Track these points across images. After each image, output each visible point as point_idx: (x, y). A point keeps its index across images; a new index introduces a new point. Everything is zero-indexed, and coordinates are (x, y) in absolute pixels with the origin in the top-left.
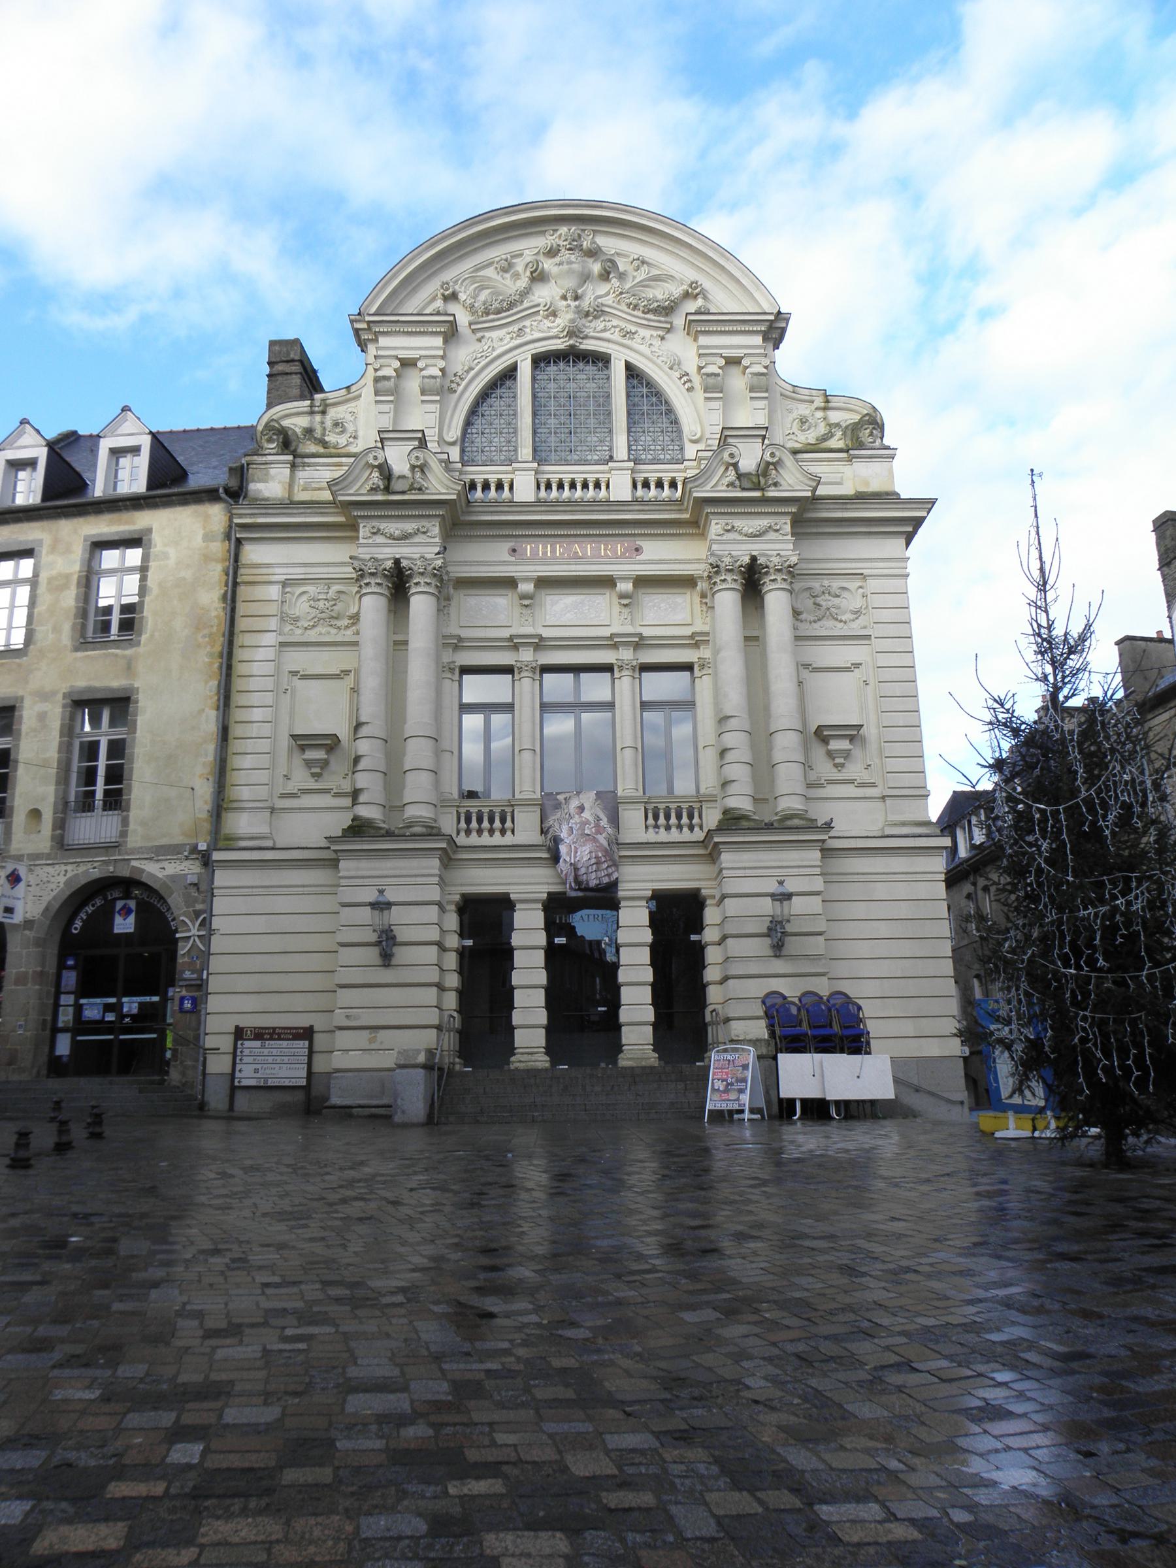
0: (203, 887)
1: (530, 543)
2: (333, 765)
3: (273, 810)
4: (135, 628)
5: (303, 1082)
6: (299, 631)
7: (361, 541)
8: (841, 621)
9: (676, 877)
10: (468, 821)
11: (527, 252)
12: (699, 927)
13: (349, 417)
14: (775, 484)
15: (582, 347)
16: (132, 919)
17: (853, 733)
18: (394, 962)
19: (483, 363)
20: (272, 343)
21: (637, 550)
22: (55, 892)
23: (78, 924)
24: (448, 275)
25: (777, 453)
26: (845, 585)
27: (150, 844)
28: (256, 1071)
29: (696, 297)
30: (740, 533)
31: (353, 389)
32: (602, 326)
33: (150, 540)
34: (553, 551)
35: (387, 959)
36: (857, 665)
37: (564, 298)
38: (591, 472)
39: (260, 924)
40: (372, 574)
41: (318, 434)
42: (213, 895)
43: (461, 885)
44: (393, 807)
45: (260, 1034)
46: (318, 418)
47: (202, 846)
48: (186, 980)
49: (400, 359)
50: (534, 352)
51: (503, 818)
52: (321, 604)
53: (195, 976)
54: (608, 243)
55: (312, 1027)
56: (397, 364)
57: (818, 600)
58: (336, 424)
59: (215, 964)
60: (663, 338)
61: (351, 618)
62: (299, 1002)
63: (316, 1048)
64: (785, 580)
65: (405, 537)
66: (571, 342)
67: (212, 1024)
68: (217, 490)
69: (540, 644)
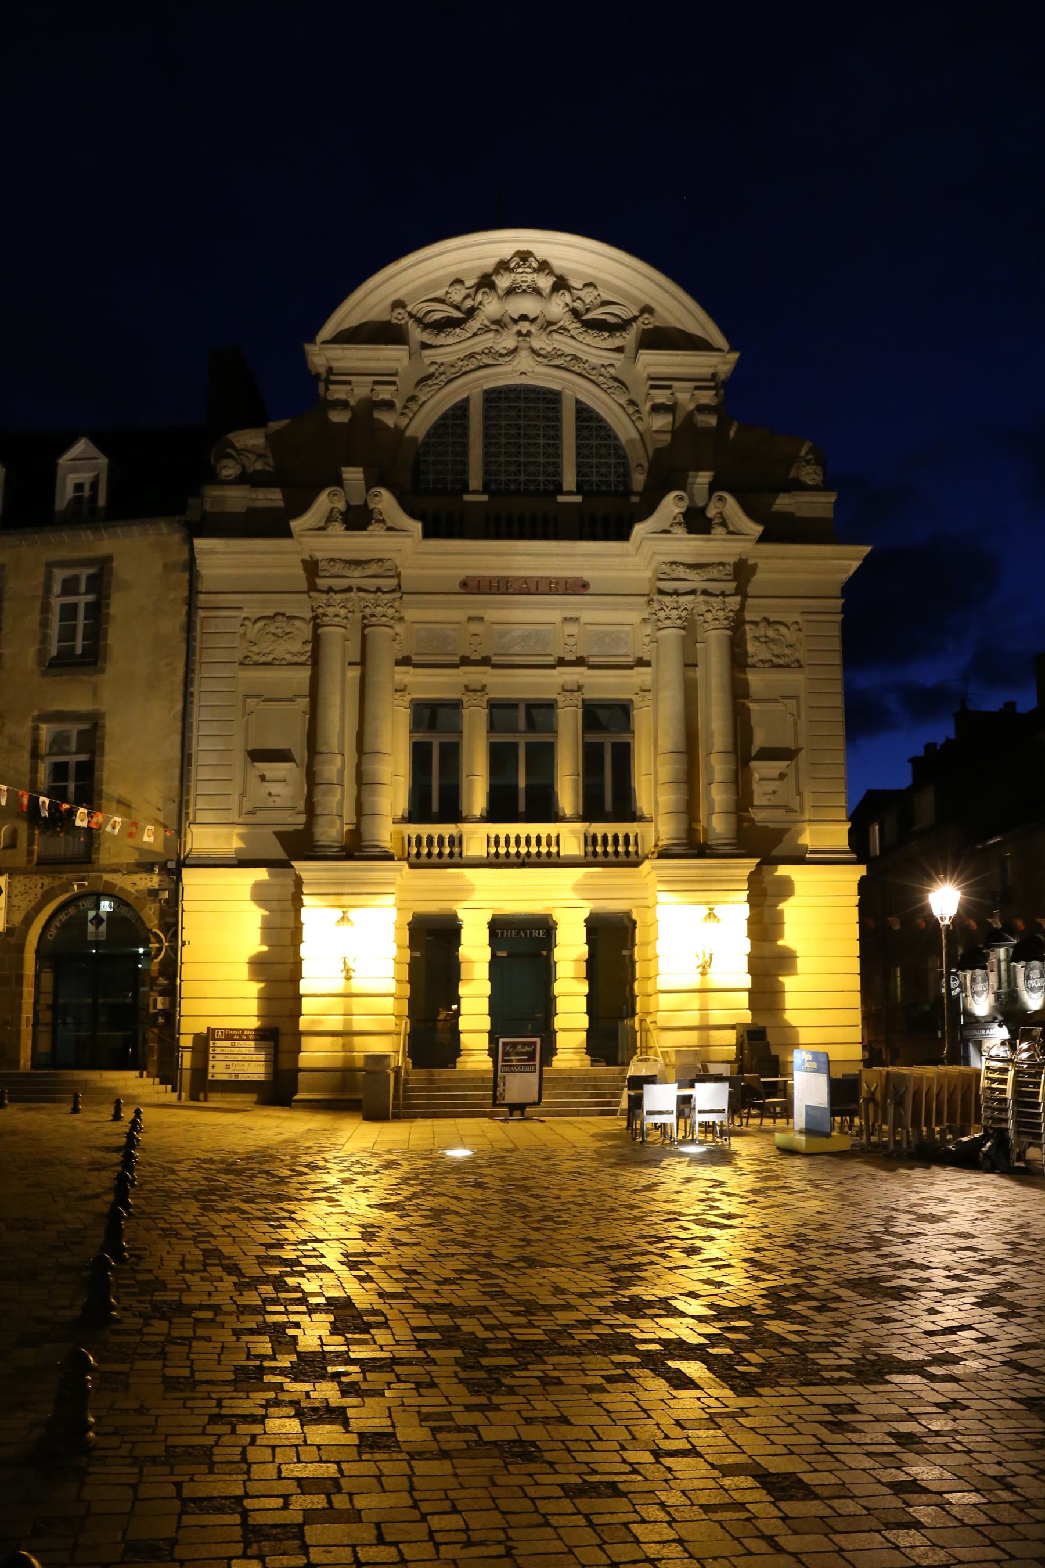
16: (103, 927)
22: (33, 903)
23: (53, 931)
28: (228, 1067)
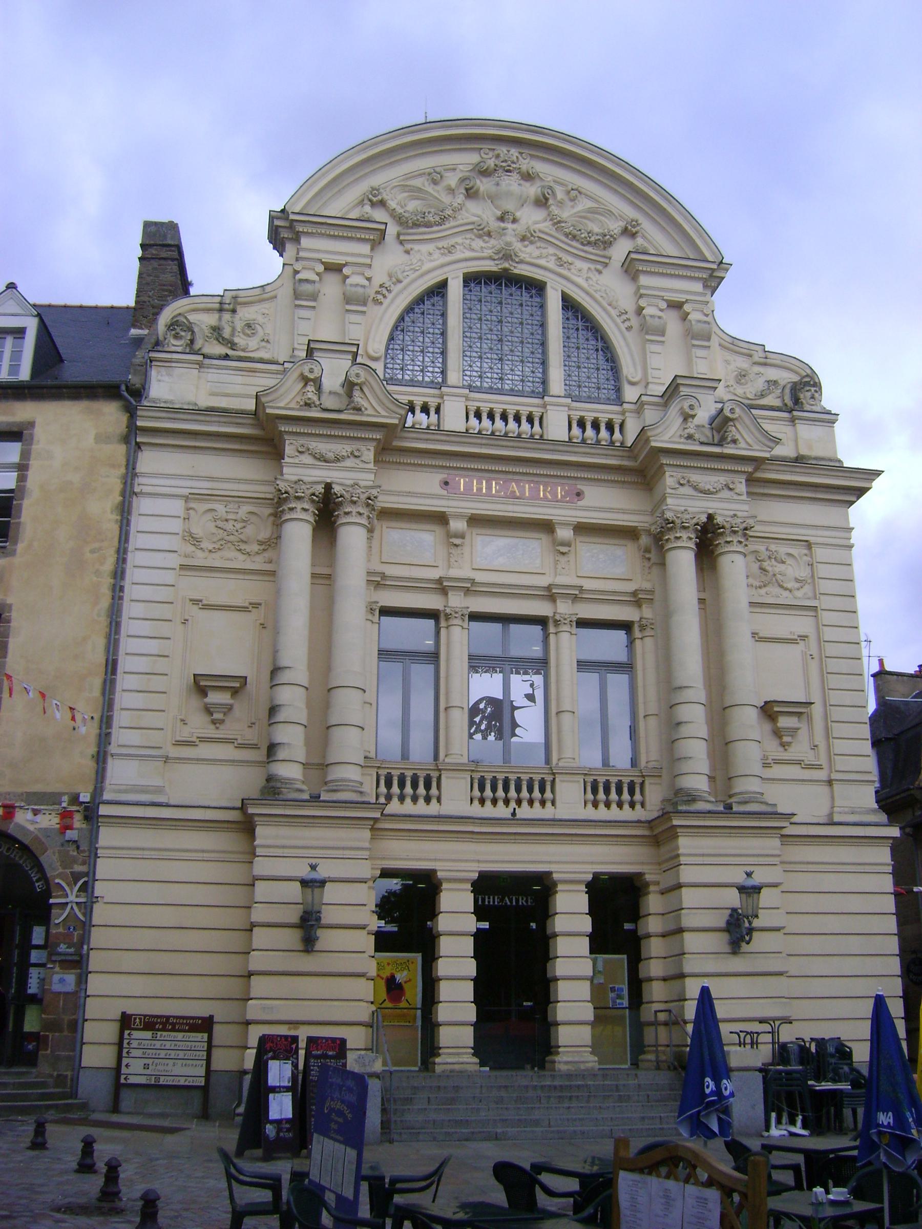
0: (84, 846)
1: (464, 477)
2: (237, 711)
3: (167, 759)
4: (11, 534)
5: (201, 1082)
6: (199, 554)
7: (287, 460)
8: (786, 589)
9: (615, 859)
10: (389, 784)
11: (461, 167)
12: (636, 915)
13: (260, 319)
14: (734, 441)
15: (516, 271)
17: (800, 709)
18: (319, 946)
19: (413, 276)
20: (147, 225)
21: (578, 494)
24: (377, 180)
25: (737, 410)
26: (791, 551)
27: (20, 790)
29: (633, 235)
30: (695, 488)
31: (268, 289)
32: (537, 253)
33: (32, 437)
34: (489, 488)
35: (309, 943)
36: (803, 638)
37: (502, 219)
38: (527, 405)
39: (151, 893)
40: (298, 498)
41: (226, 333)
42: (96, 856)
43: (383, 859)
44: (319, 766)
45: (152, 1023)
46: (227, 316)
47: (85, 797)
48: (60, 954)
49: (323, 263)
50: (466, 271)
51: (427, 783)
52: (229, 526)
53: (72, 950)
54: (547, 171)
55: (211, 1017)
56: (321, 268)
57: (765, 565)
58: (249, 326)
59: (97, 937)
60: (600, 272)
61: (261, 543)
62: (195, 987)
63: (215, 1043)
64: (740, 542)
65: (337, 459)
66: (506, 265)
67: (93, 1008)
68: (118, 387)
69: (470, 588)
